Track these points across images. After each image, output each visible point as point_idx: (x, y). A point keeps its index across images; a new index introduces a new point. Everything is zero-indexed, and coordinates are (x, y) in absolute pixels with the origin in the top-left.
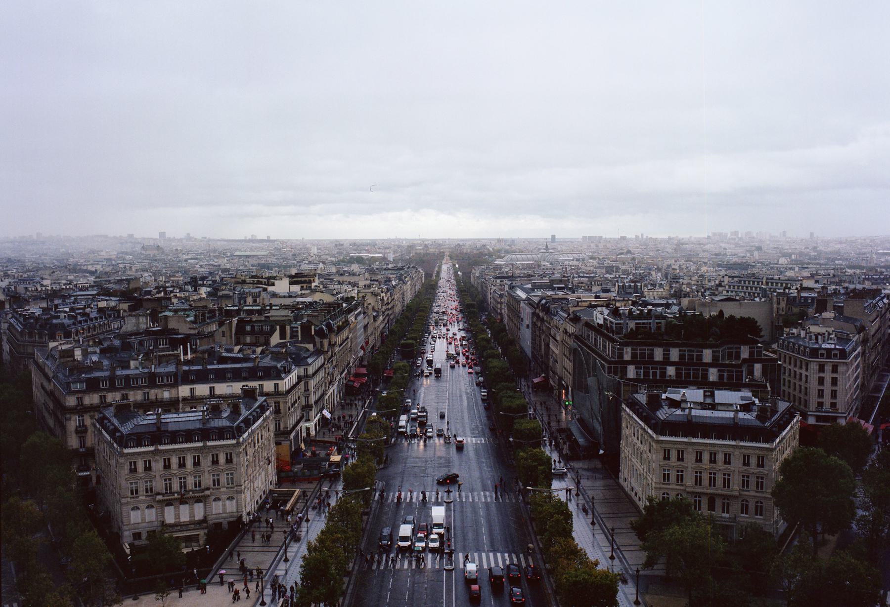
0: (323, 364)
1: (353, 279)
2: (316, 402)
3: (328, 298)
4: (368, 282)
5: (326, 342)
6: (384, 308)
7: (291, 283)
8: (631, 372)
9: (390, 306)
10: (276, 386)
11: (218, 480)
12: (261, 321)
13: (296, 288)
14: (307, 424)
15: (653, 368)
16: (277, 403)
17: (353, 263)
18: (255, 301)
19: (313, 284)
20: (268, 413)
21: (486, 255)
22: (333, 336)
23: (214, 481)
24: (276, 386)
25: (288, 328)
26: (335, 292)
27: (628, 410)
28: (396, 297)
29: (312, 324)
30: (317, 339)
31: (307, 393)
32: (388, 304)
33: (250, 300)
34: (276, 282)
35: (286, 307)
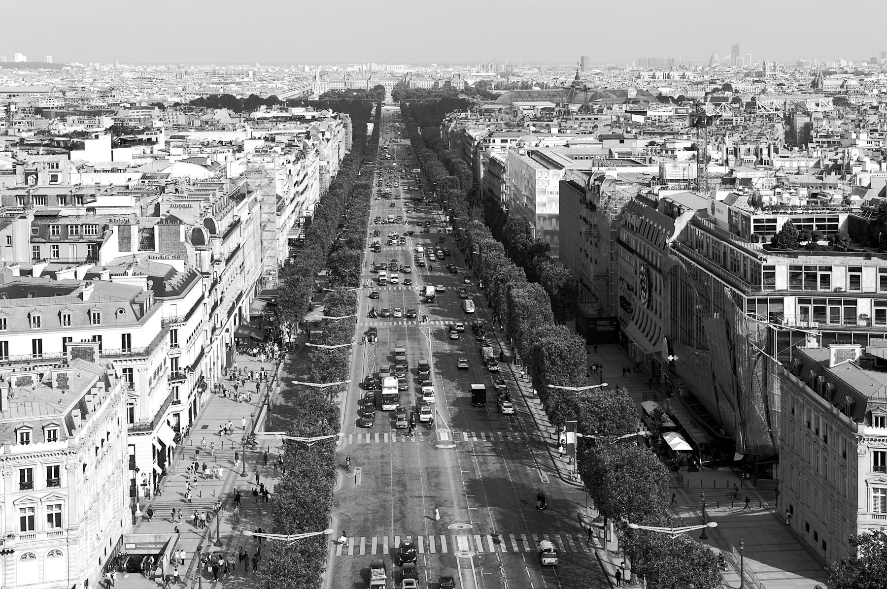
0: (203, 297)
1: (226, 136)
2: (192, 368)
3: (198, 173)
4: (261, 143)
5: (206, 255)
6: (293, 190)
7: (114, 145)
8: (790, 309)
9: (300, 188)
10: (126, 340)
11: (31, 518)
12: (78, 216)
13: (125, 155)
14: (176, 408)
15: (831, 302)
16: (129, 373)
17: (216, 106)
18: (54, 178)
19: (156, 147)
20: (118, 388)
21: (462, 92)
22: (217, 243)
23: (23, 519)
24: (126, 340)
25: (134, 230)
26: (209, 162)
27: (794, 378)
28: (309, 171)
29: (181, 222)
30: (190, 249)
31: (174, 351)
32: (297, 184)
33: (44, 177)
34: (87, 142)
35: (126, 190)
